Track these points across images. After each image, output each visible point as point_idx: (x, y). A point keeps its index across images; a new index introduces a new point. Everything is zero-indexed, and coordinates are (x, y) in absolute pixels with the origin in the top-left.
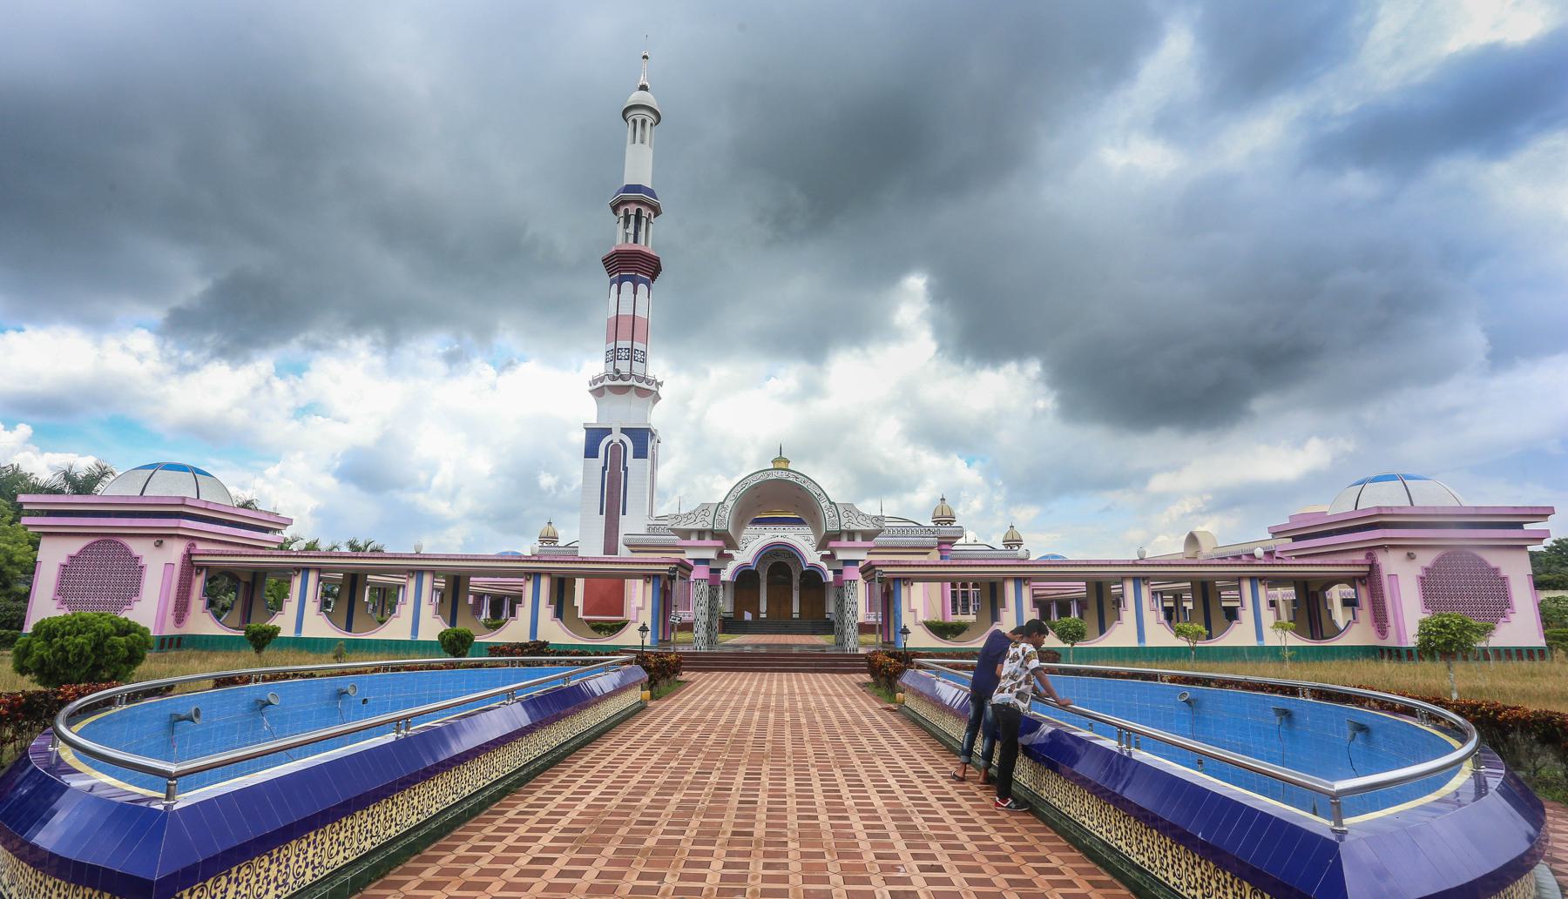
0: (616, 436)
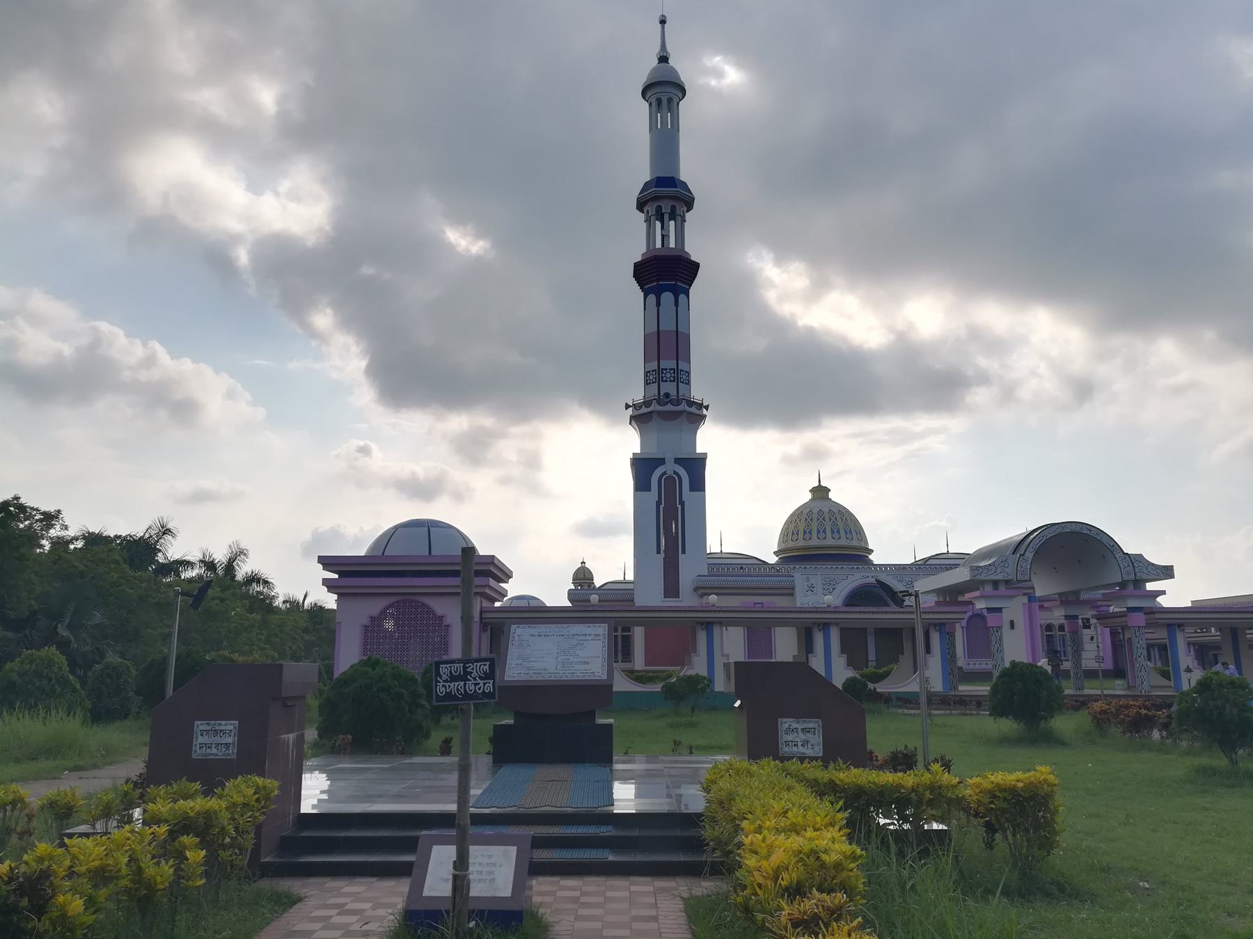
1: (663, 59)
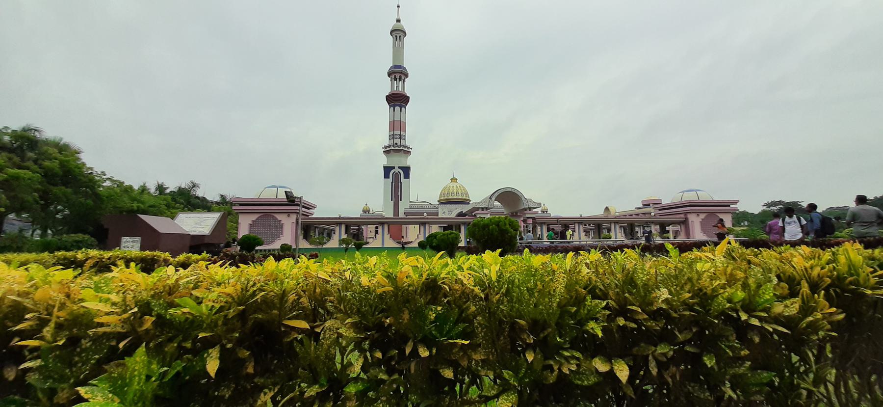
0: (397, 170)
1: (398, 21)
